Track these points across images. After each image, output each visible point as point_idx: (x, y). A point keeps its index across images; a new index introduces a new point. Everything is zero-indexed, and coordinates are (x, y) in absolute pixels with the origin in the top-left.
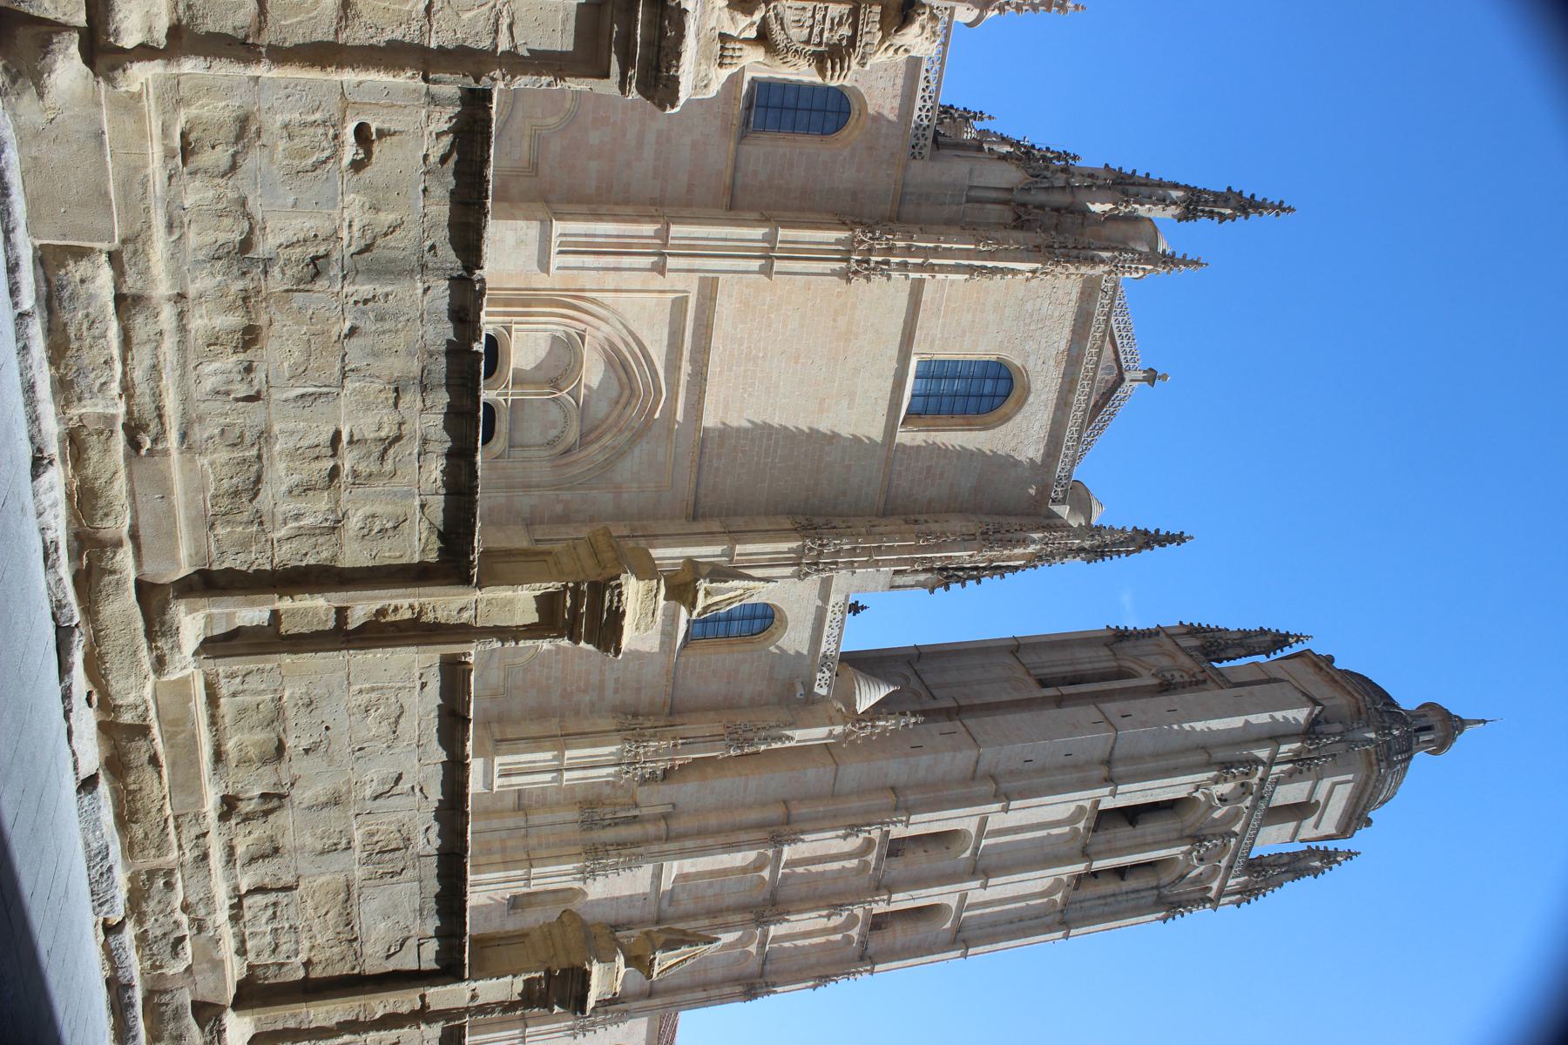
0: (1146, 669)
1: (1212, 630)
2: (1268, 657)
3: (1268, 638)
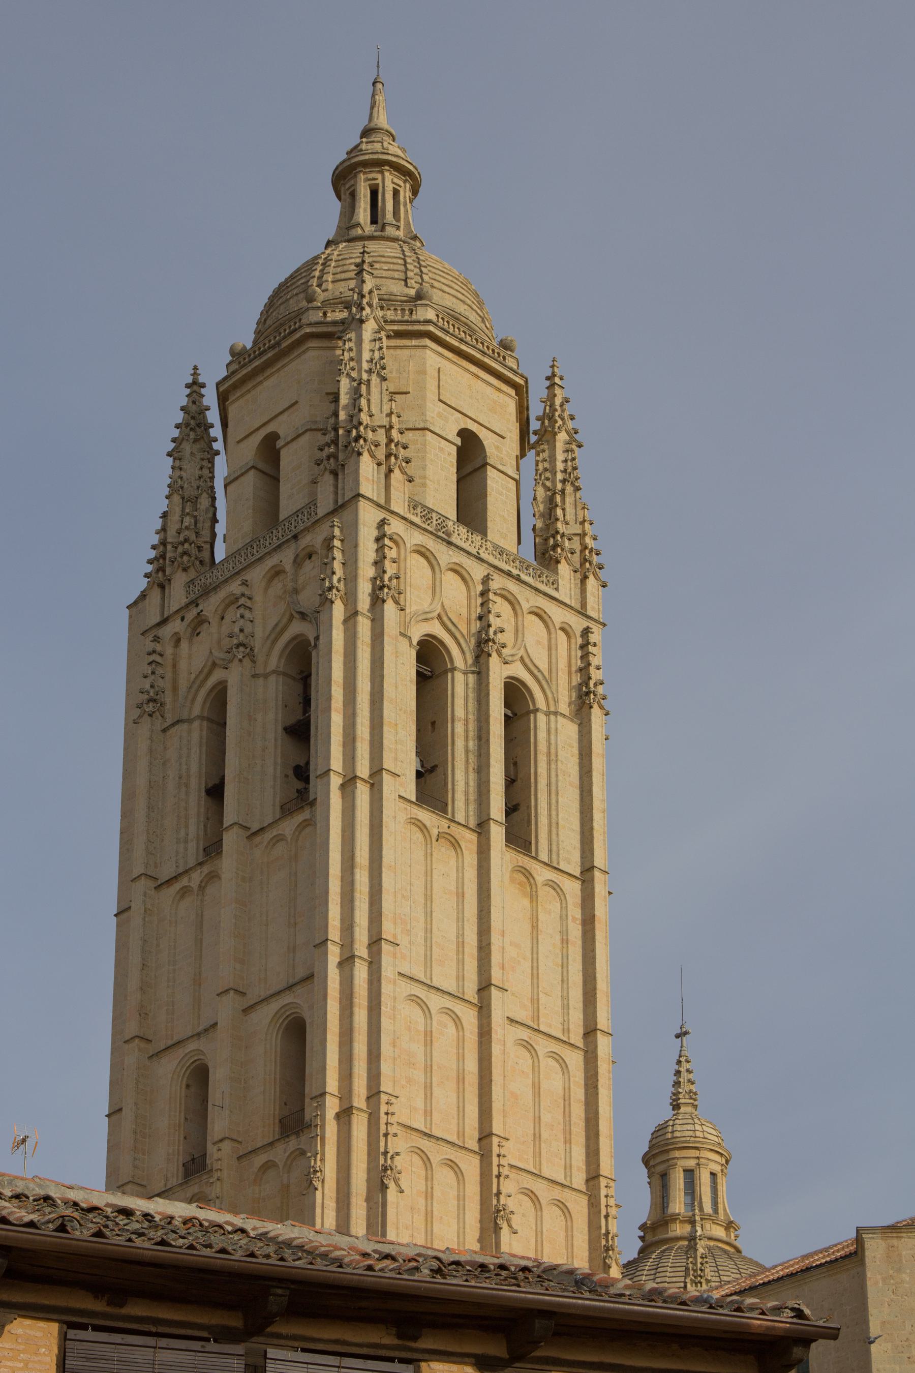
0: (210, 673)
1: (163, 543)
2: (217, 453)
3: (187, 447)
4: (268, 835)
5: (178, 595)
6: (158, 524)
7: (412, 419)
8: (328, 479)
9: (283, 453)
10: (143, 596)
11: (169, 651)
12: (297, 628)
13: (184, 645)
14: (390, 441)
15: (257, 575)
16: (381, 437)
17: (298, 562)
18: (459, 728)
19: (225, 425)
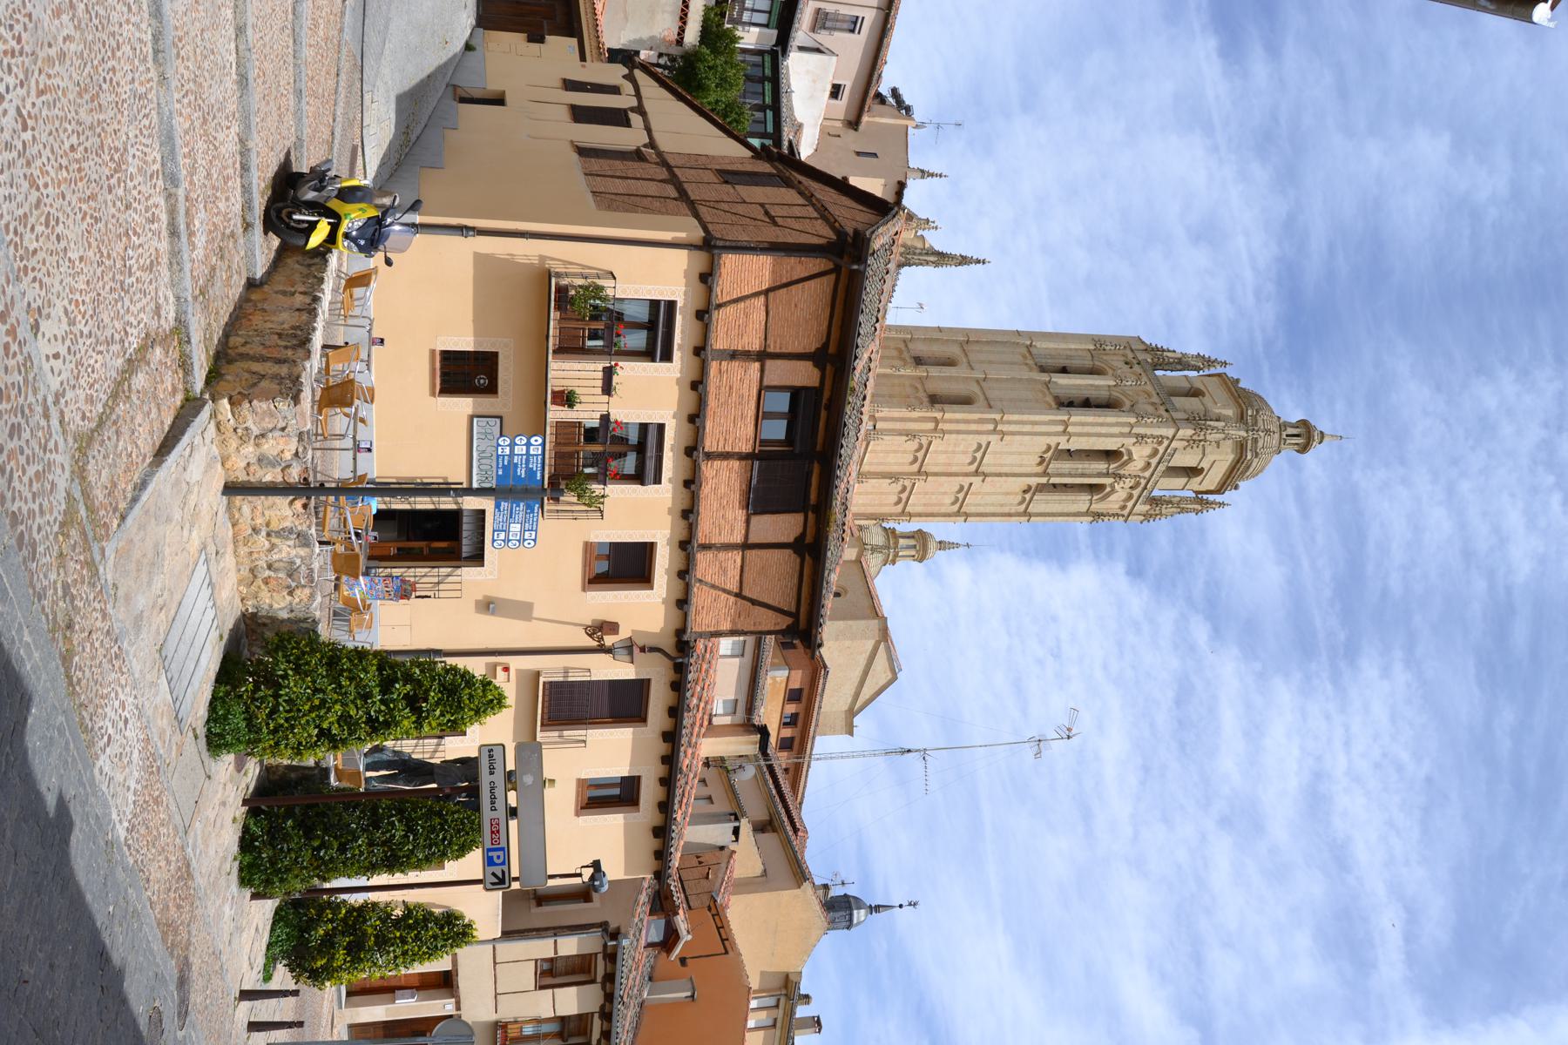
4: (1046, 390)
5: (1141, 356)
6: (1171, 349)
7: (1208, 450)
8: (1186, 417)
9: (1197, 399)
10: (1143, 342)
11: (1121, 352)
12: (1128, 404)
13: (1123, 358)
14: (1200, 441)
15: (1149, 388)
16: (1202, 438)
17: (1153, 404)
18: (1086, 466)
19: (1209, 376)
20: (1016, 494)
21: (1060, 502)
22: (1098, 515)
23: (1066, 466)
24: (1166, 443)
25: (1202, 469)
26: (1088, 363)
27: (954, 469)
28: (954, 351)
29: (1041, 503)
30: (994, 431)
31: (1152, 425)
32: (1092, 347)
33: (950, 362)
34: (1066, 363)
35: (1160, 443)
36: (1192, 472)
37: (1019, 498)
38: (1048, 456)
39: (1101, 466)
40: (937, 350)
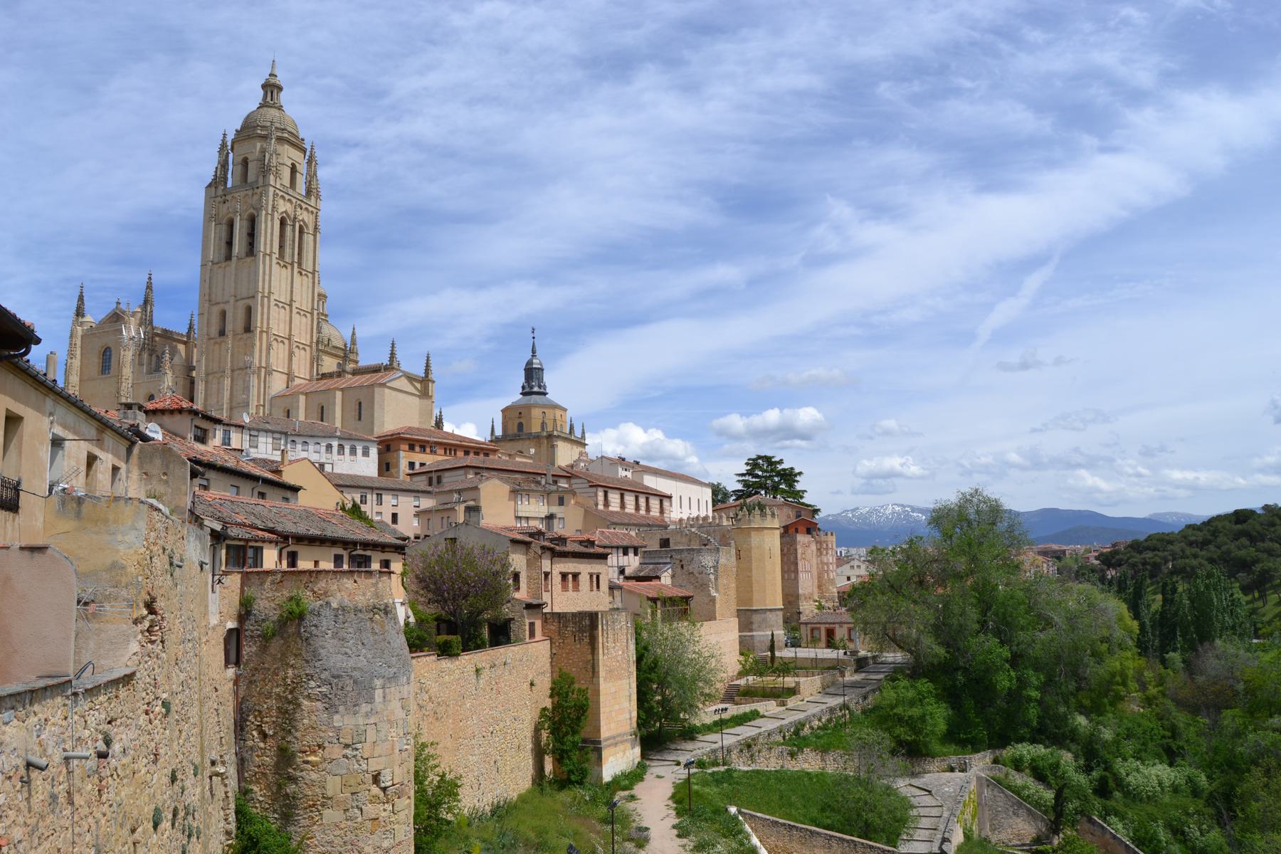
20: (302, 280)
21: (307, 252)
22: (316, 228)
23: (288, 250)
24: (277, 191)
25: (293, 164)
26: (224, 228)
27: (288, 318)
28: (216, 310)
29: (308, 265)
30: (269, 297)
31: (267, 201)
32: (214, 223)
33: (223, 314)
34: (224, 241)
35: (277, 195)
36: (294, 170)
37: (304, 277)
38: (282, 263)
39: (289, 229)
40: (215, 320)
